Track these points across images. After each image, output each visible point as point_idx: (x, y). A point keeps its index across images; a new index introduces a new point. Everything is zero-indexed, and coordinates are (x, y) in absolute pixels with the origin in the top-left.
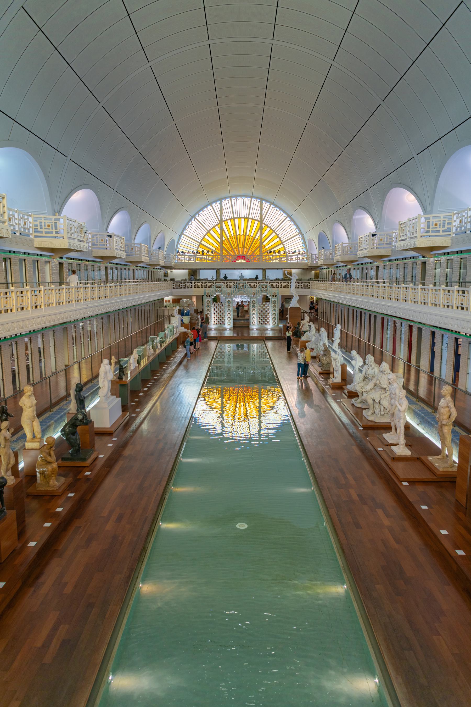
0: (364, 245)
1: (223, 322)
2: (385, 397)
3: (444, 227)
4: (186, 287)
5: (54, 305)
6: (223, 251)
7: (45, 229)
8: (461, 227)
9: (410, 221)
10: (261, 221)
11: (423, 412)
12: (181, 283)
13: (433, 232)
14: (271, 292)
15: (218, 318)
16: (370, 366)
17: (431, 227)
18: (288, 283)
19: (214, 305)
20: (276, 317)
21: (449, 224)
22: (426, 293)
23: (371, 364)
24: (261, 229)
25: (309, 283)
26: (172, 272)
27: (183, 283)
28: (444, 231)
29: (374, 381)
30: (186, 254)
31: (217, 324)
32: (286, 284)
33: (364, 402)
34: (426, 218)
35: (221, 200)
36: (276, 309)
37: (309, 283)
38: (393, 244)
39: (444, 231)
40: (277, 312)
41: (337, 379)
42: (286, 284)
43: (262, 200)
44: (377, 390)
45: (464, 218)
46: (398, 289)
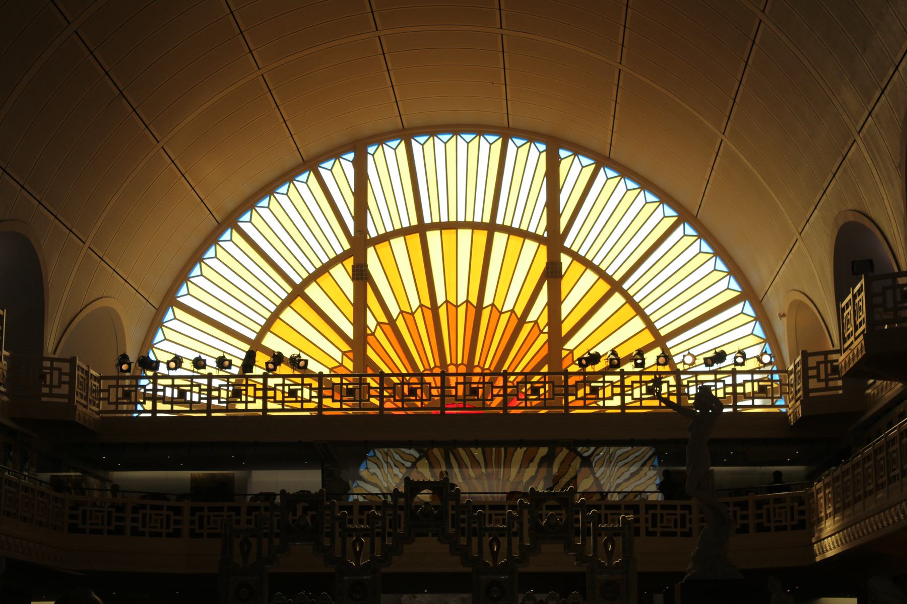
30: (163, 369)
32: (679, 512)
42: (679, 512)
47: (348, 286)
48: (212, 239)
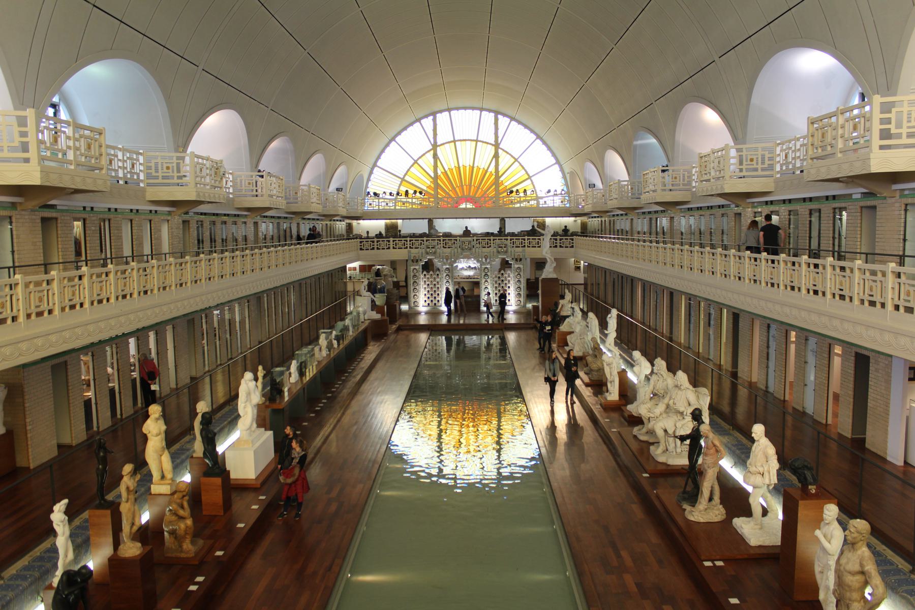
0: (650, 185)
1: (438, 301)
2: (683, 425)
3: (763, 163)
4: (381, 248)
5: (173, 288)
6: (439, 191)
7: (162, 172)
8: (787, 164)
9: (714, 153)
10: (497, 145)
11: (740, 447)
12: (373, 242)
13: (747, 170)
14: (513, 254)
15: (430, 296)
16: (660, 376)
17: (745, 163)
18: (540, 239)
19: (425, 275)
20: (522, 293)
21: (771, 159)
22: (740, 263)
23: (662, 373)
24: (496, 156)
25: (572, 240)
26: (359, 223)
27: (376, 242)
28: (763, 170)
29: (666, 401)
30: (381, 196)
31: (429, 304)
32: (537, 240)
33: (651, 432)
34: (738, 150)
35: (434, 114)
36: (522, 280)
37: (572, 240)
38: (694, 184)
39: (763, 170)
40: (523, 285)
41: (613, 395)
43: (497, 113)
44: (670, 414)
45: (790, 151)
46: (702, 254)
47: (432, 160)
48: (388, 145)
